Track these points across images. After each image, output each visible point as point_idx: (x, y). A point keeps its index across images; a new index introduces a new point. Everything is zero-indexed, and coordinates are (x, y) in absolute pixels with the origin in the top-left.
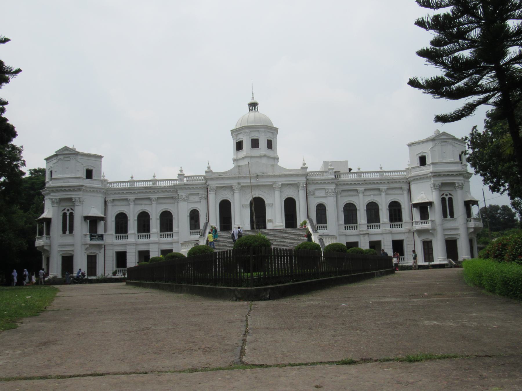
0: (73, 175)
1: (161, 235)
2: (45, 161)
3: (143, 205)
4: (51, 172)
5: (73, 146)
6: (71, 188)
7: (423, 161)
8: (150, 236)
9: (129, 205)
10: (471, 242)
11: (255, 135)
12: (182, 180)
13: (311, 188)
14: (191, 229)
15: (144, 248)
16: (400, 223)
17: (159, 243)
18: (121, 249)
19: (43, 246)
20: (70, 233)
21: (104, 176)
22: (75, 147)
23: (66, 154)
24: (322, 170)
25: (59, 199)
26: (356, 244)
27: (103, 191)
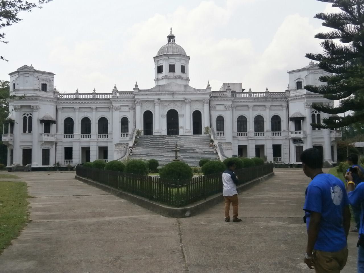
0: (31, 88)
1: (99, 136)
2: (9, 75)
3: (86, 113)
4: (14, 84)
5: (32, 66)
6: (30, 98)
7: (299, 85)
8: (90, 136)
9: (75, 111)
10: (332, 147)
11: (172, 61)
12: (115, 94)
13: (214, 103)
14: (121, 132)
15: (85, 145)
16: (279, 132)
17: (97, 142)
18: (68, 145)
19: (8, 142)
20: (29, 132)
21: (55, 89)
22: (33, 66)
23: (25, 71)
24: (222, 90)
25: (21, 106)
26: (246, 146)
27: (54, 100)
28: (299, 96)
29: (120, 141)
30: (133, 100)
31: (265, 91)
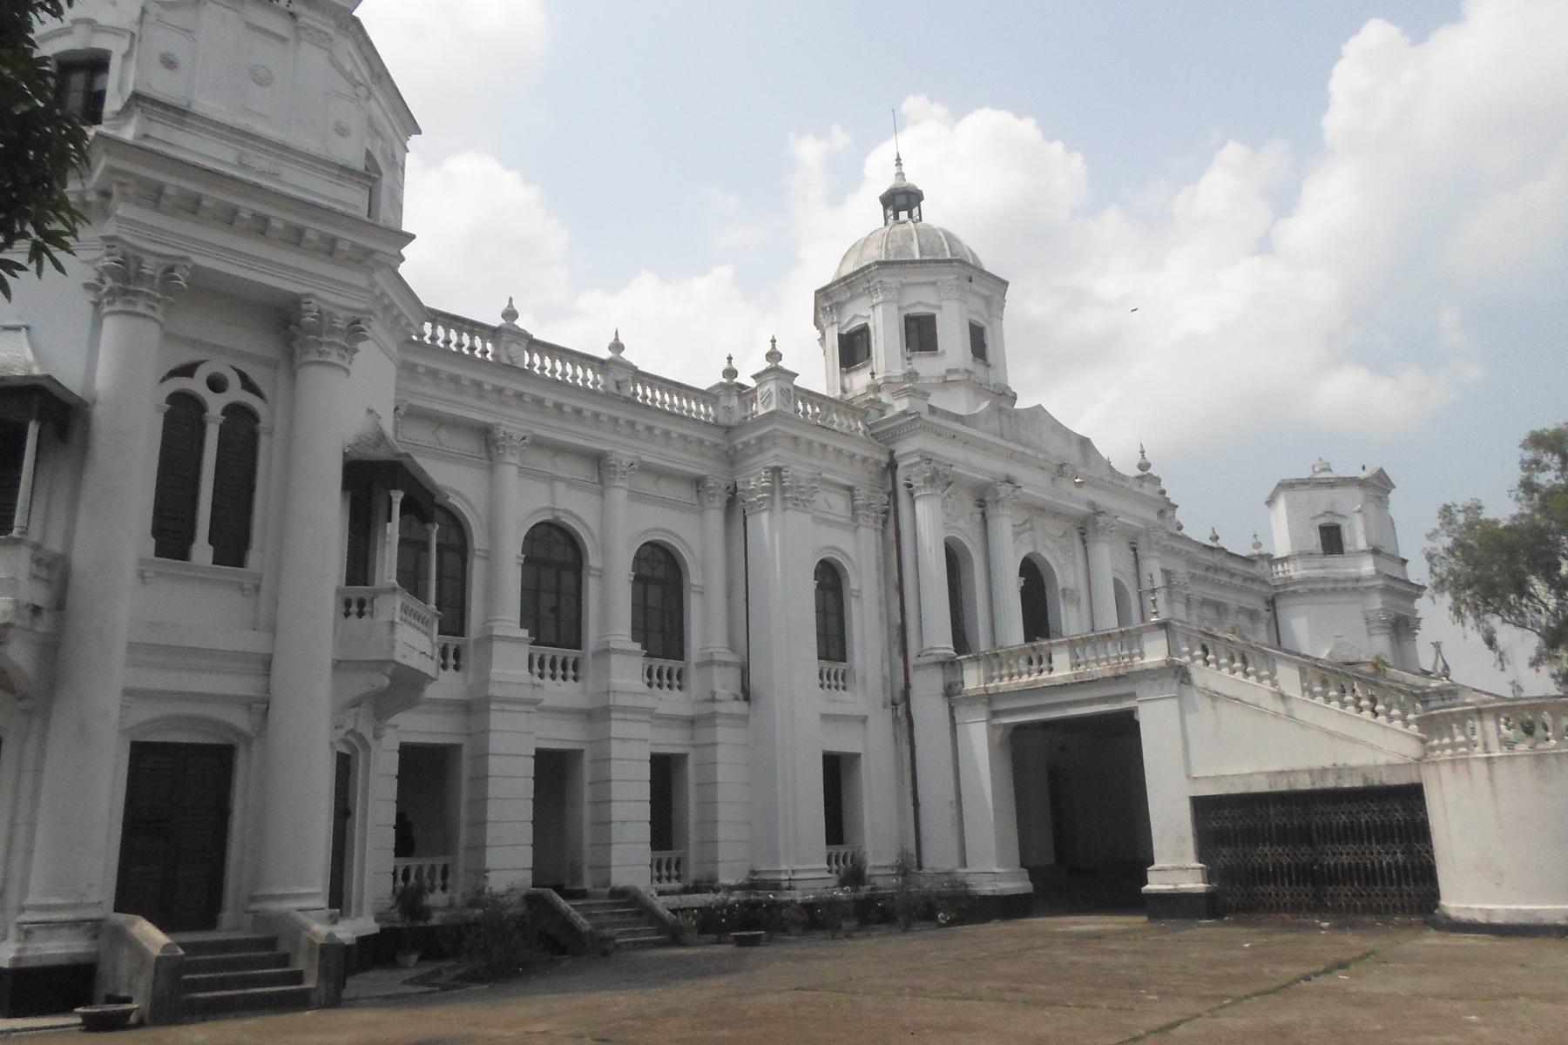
3: (560, 487)
7: (1332, 539)
15: (560, 736)
20: (218, 559)
28: (1345, 580)
29: (825, 717)
30: (878, 463)
31: (1209, 543)
